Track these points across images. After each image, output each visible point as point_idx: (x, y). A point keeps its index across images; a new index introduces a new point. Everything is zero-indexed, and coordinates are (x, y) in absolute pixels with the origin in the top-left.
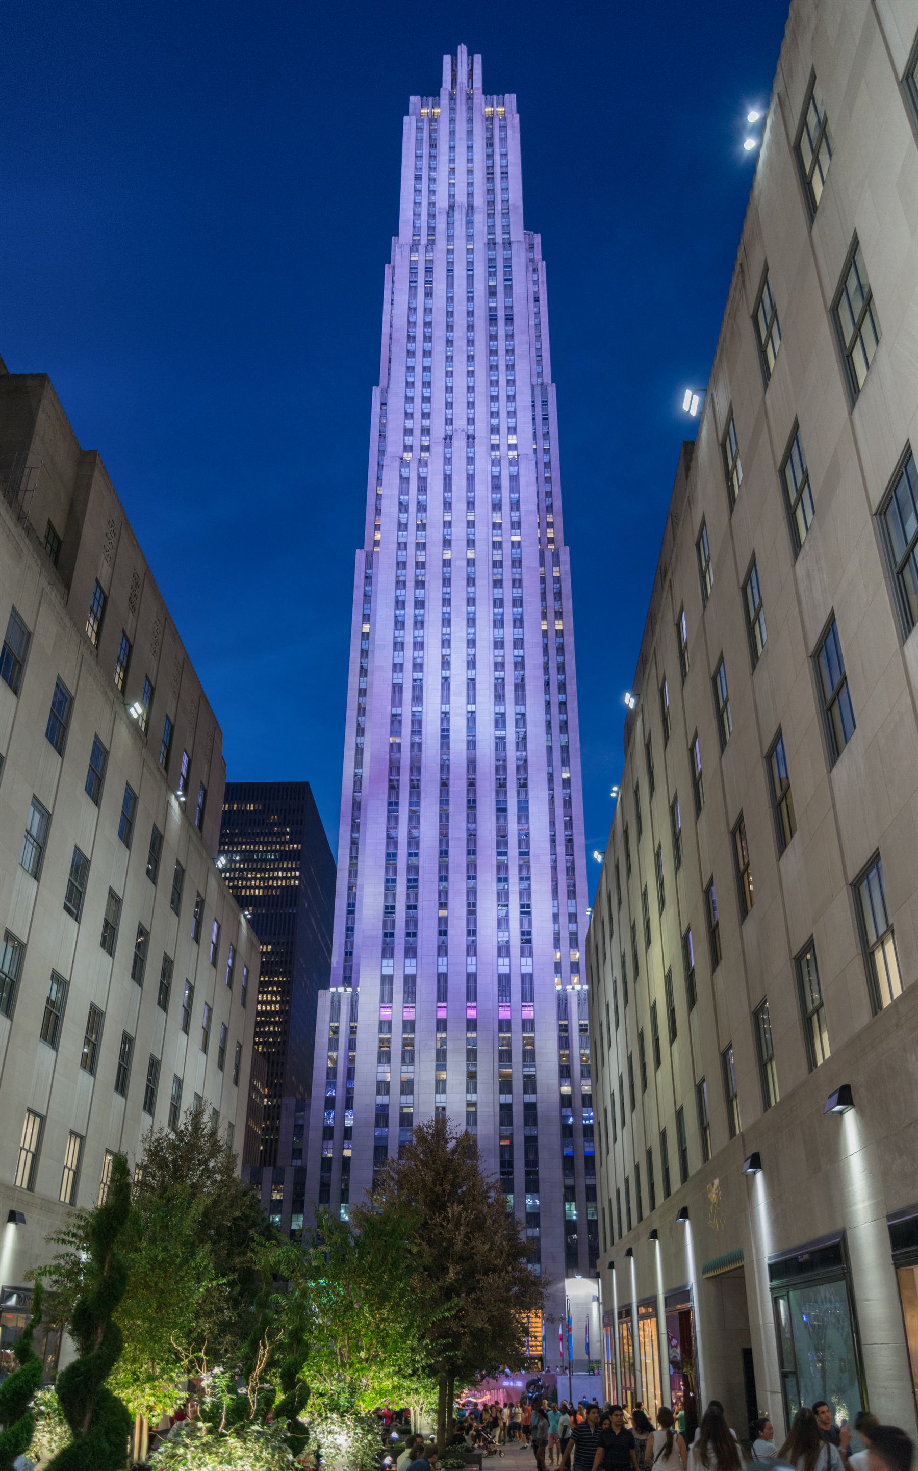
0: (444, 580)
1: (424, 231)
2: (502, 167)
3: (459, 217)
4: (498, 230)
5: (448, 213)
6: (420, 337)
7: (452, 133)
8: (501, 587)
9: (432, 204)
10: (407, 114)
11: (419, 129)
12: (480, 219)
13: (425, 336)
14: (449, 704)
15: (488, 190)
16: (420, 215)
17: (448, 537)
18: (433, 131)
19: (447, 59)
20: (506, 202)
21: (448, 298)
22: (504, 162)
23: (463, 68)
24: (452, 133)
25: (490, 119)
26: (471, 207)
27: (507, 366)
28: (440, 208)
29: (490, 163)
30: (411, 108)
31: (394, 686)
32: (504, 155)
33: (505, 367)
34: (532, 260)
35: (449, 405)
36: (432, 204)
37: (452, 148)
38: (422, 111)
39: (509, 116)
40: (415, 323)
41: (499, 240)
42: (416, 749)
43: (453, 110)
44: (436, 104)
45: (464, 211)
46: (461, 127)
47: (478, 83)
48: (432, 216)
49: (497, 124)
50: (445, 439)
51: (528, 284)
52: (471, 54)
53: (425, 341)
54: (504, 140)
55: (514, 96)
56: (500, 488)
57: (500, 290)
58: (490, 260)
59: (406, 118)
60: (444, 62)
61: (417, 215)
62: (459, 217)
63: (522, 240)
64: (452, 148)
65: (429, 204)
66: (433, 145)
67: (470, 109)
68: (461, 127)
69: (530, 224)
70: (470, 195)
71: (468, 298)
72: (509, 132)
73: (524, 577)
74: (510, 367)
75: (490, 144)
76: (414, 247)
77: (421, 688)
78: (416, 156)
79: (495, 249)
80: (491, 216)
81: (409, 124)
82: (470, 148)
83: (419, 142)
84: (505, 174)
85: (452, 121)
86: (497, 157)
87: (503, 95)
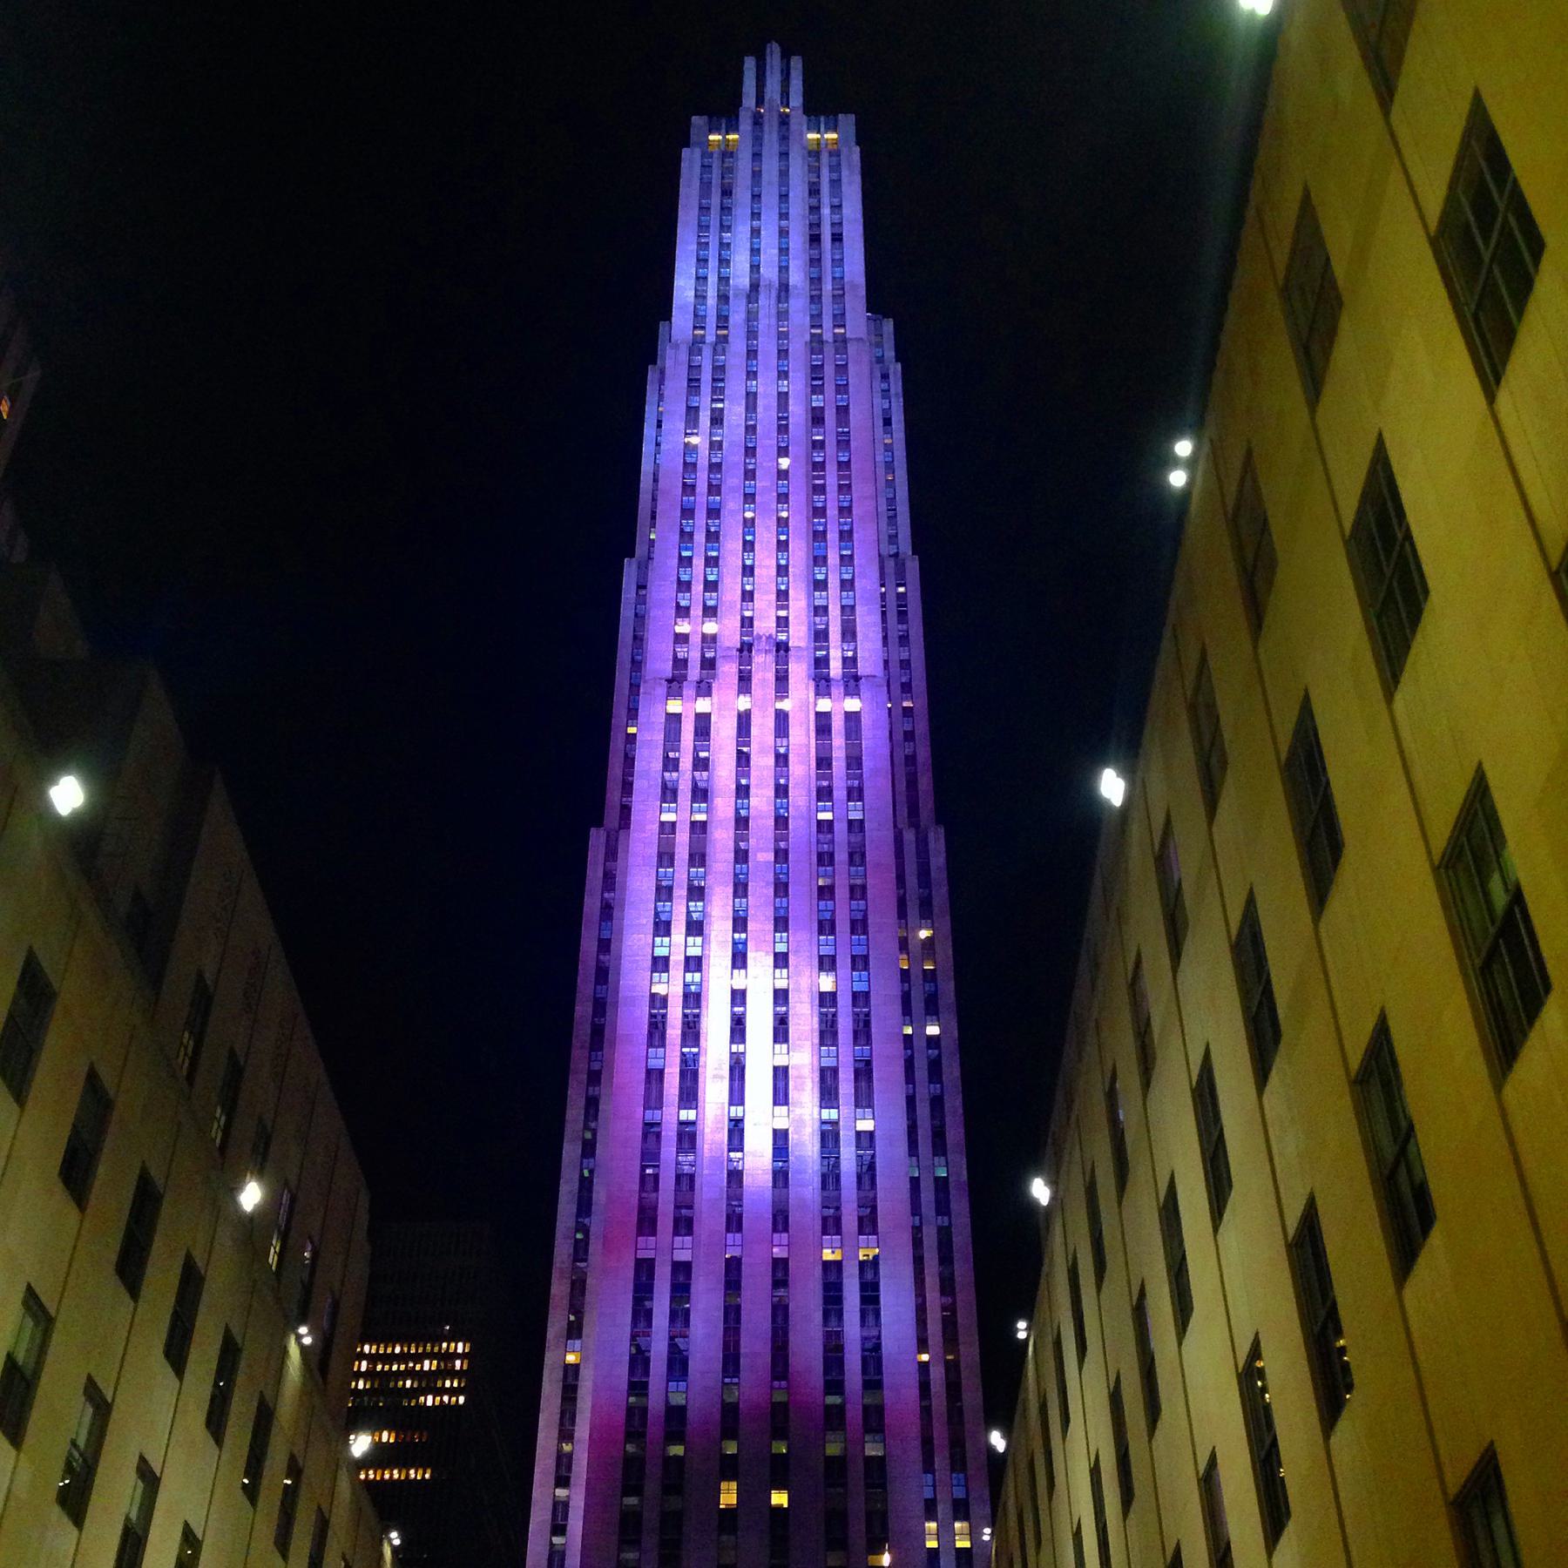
0: (735, 885)
1: (711, 321)
2: (833, 224)
3: (766, 303)
4: (827, 321)
5: (749, 297)
6: (702, 487)
7: (756, 175)
8: (832, 898)
9: (724, 280)
10: (688, 146)
11: (706, 168)
12: (798, 306)
13: (710, 485)
14: (742, 1104)
15: (811, 260)
16: (705, 297)
17: (743, 813)
18: (727, 171)
19: (750, 64)
20: (839, 281)
21: (747, 427)
22: (836, 218)
23: (774, 83)
24: (756, 175)
25: (815, 153)
26: (784, 288)
27: (841, 532)
28: (736, 289)
29: (815, 272)
30: (693, 138)
31: (649, 1072)
32: (836, 208)
33: (837, 535)
34: (880, 360)
35: (748, 596)
36: (724, 280)
37: (756, 197)
38: (711, 137)
39: (844, 150)
40: (695, 465)
41: (828, 337)
42: (685, 1186)
43: (758, 140)
44: (733, 127)
45: (774, 293)
46: (770, 167)
47: (796, 100)
48: (723, 298)
49: (825, 158)
50: (741, 650)
51: (873, 407)
52: (786, 56)
53: (710, 493)
54: (836, 184)
55: (852, 117)
56: (830, 731)
57: (830, 417)
58: (814, 368)
59: (685, 152)
60: (746, 66)
61: (700, 297)
62: (766, 303)
63: (864, 336)
64: (756, 197)
65: (720, 279)
66: (727, 192)
67: (784, 138)
68: (770, 167)
69: (876, 303)
70: (783, 269)
71: (779, 426)
72: (845, 173)
73: (870, 882)
74: (846, 536)
75: (814, 191)
76: (696, 345)
77: (695, 1074)
78: (701, 208)
79: (821, 352)
80: (816, 299)
81: (690, 160)
82: (784, 197)
83: (705, 187)
84: (837, 238)
85: (757, 156)
86: (826, 211)
87: (836, 115)
